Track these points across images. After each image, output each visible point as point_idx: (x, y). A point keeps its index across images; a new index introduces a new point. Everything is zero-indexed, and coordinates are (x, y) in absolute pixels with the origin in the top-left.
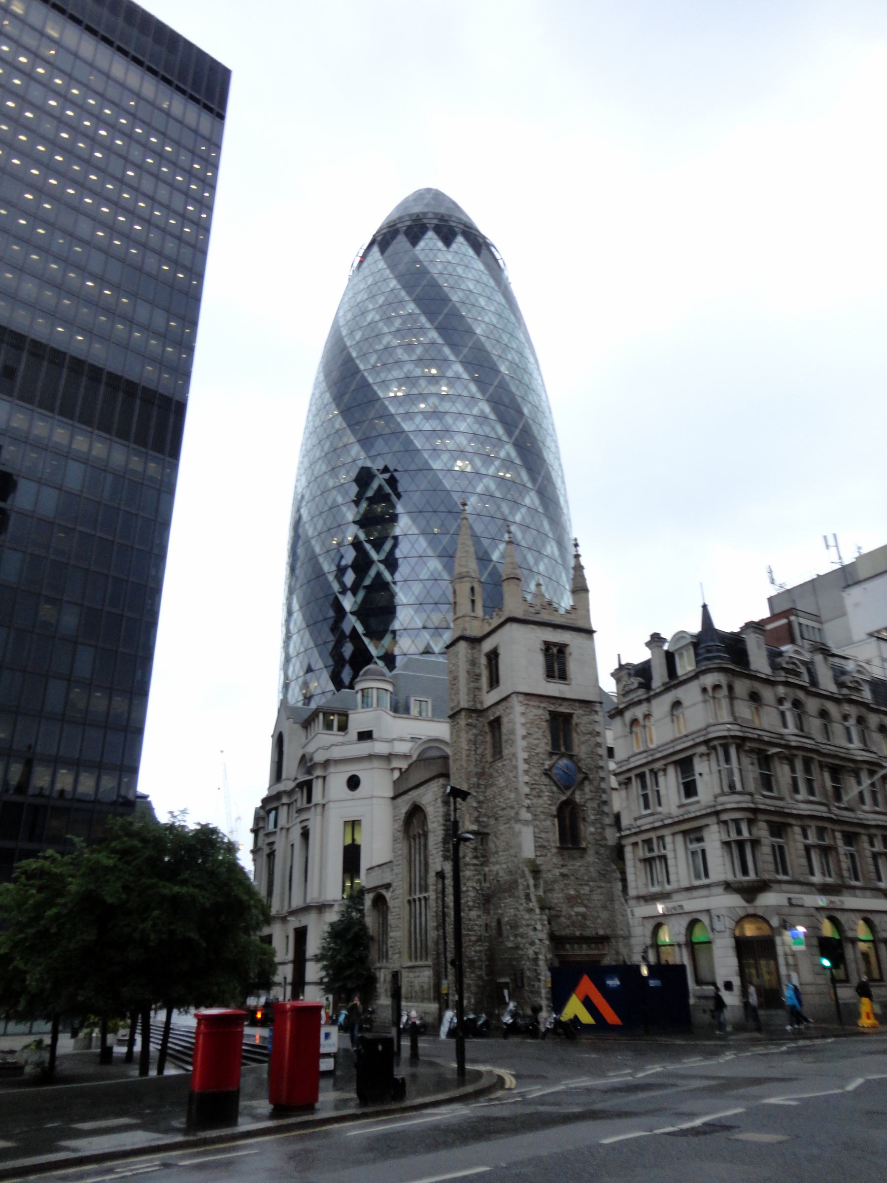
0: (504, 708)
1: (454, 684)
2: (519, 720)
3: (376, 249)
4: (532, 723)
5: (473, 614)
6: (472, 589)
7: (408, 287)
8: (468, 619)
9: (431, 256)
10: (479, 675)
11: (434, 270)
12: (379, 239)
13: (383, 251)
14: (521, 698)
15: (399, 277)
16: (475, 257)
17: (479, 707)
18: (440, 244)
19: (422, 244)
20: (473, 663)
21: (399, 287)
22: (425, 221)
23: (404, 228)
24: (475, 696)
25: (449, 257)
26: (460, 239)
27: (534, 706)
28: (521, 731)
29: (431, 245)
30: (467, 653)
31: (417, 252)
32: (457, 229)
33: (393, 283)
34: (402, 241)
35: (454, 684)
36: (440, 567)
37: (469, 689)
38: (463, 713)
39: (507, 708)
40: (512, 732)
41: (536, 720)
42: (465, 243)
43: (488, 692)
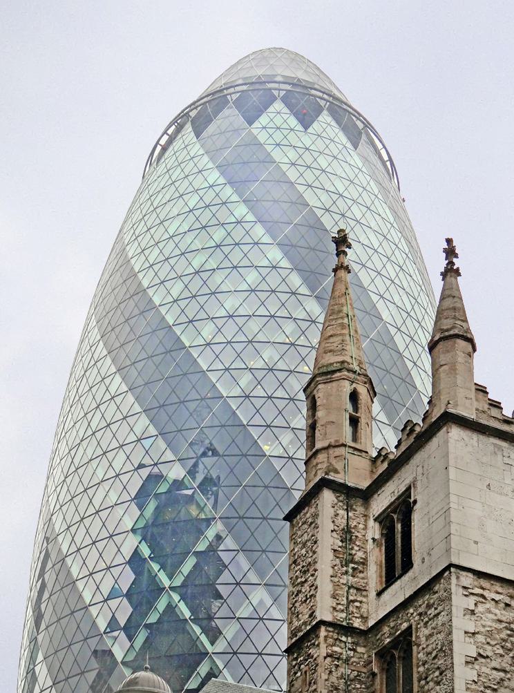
0: (420, 610)
1: (302, 584)
2: (461, 624)
3: (188, 128)
4: (489, 634)
5: (353, 445)
6: (354, 397)
8: (341, 451)
9: (278, 137)
10: (364, 563)
12: (193, 114)
14: (467, 579)
16: (349, 145)
17: (357, 623)
18: (293, 122)
19: (264, 120)
20: (347, 535)
24: (350, 602)
25: (307, 141)
27: (496, 602)
28: (463, 649)
29: (278, 121)
30: (337, 515)
31: (255, 132)
34: (230, 117)
35: (302, 584)
37: (337, 585)
38: (323, 632)
39: (429, 606)
40: (446, 649)
41: (499, 631)
42: (333, 123)
43: (379, 594)
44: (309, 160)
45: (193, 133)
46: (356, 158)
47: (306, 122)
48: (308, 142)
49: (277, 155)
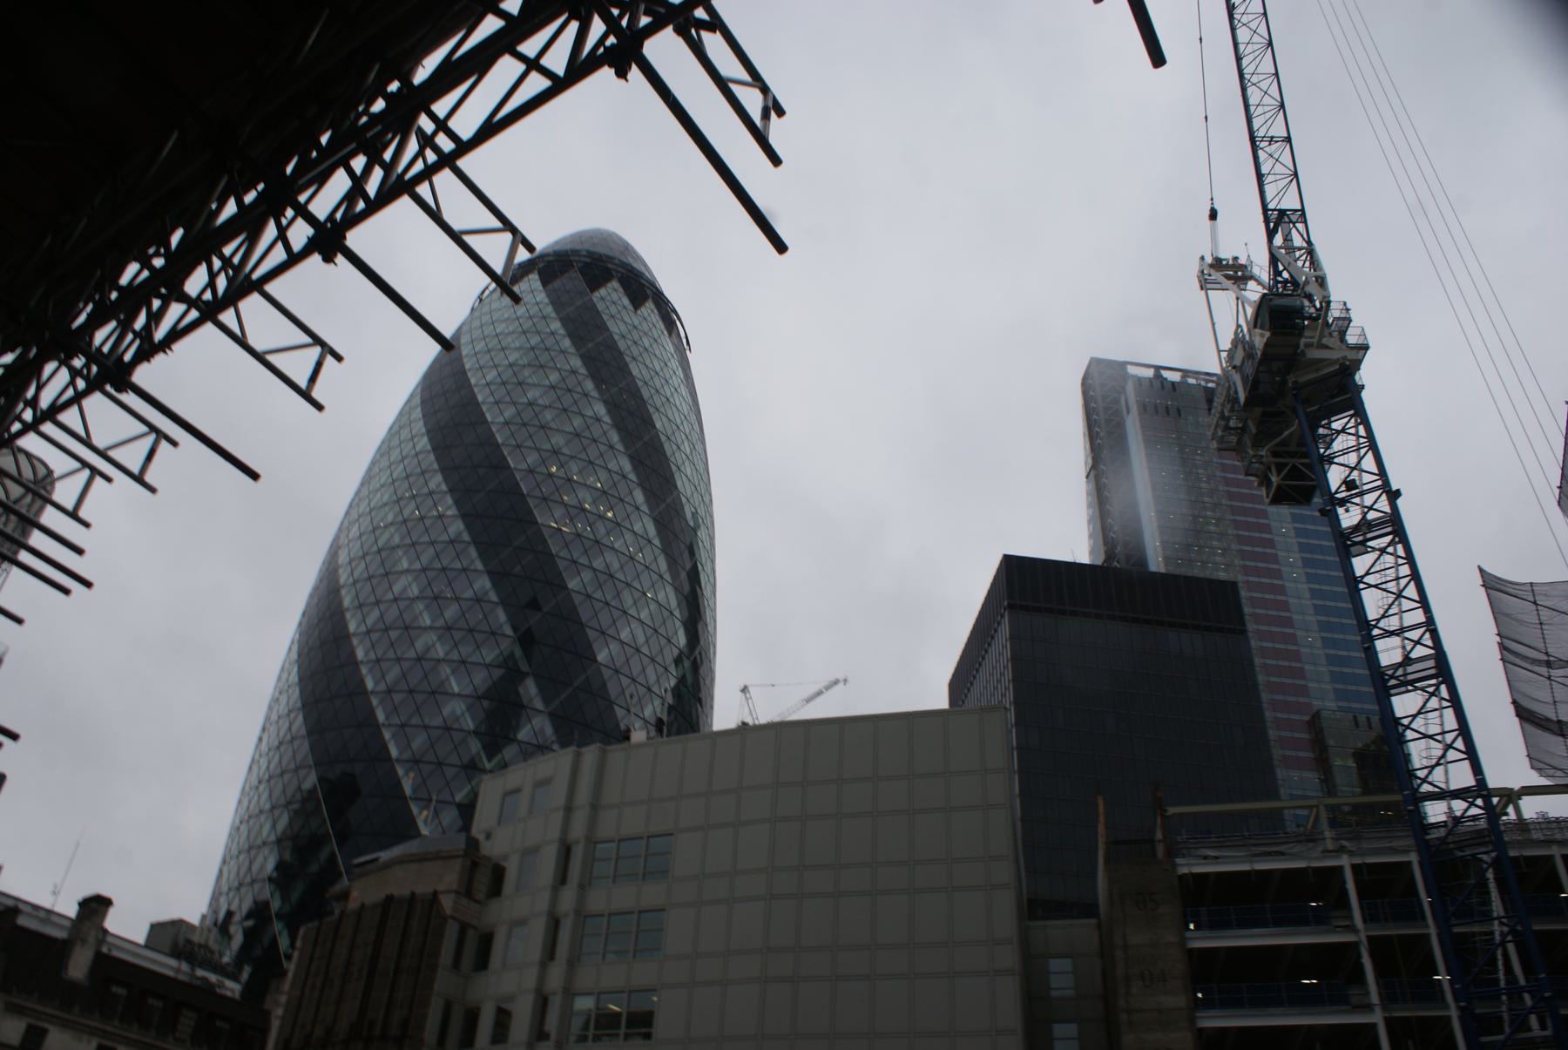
7: (576, 339)
9: (613, 310)
11: (615, 328)
13: (545, 283)
15: (565, 321)
16: (665, 332)
18: (626, 301)
19: (603, 292)
21: (562, 331)
22: (609, 266)
23: (580, 265)
26: (650, 305)
29: (615, 296)
31: (594, 299)
32: (648, 291)
33: (556, 325)
34: (572, 281)
36: (549, 730)
44: (636, 337)
45: (539, 283)
46: (670, 344)
47: (637, 302)
48: (636, 322)
49: (610, 324)
